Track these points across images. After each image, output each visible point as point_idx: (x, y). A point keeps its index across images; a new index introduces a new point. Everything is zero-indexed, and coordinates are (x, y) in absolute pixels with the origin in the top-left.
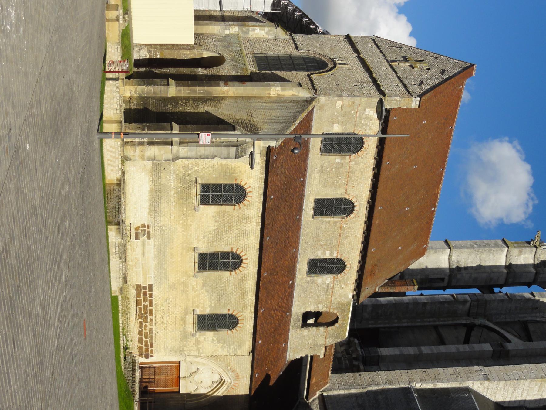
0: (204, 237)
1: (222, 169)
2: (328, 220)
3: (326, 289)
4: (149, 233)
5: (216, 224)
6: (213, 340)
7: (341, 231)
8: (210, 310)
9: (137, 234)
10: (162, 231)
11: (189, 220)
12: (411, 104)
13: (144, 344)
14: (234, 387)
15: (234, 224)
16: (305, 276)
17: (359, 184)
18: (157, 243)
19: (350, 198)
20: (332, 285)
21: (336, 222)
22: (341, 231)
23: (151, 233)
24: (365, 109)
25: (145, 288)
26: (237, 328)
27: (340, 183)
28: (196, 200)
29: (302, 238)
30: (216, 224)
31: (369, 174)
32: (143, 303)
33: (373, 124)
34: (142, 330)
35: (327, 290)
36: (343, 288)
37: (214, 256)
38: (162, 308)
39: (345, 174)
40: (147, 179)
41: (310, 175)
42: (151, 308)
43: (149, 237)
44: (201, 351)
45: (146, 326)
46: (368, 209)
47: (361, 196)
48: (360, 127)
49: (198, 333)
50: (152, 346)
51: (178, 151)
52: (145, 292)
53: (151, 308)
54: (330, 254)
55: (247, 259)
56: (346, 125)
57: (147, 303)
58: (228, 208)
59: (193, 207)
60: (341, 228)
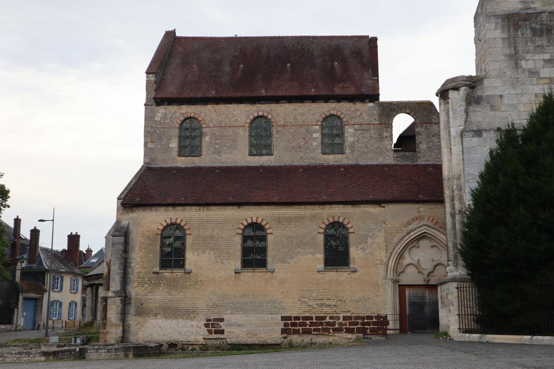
0: (223, 263)
1: (144, 248)
2: (275, 140)
3: (362, 132)
4: (215, 320)
5: (207, 252)
6: (361, 249)
7: (288, 126)
8: (319, 253)
9: (216, 332)
10: (215, 306)
11: (202, 279)
12: (151, 81)
13: (367, 327)
14: (435, 222)
15: (208, 233)
16: (344, 155)
17: (234, 116)
18: (229, 312)
19: (248, 121)
20: (356, 126)
21: (278, 132)
22: (288, 126)
23: (215, 317)
24: (156, 121)
25: (286, 325)
26: (345, 223)
27: (232, 134)
28: (178, 273)
29: (296, 163)
30: (207, 252)
31: (222, 107)
32: (308, 327)
33: (170, 112)
34: (345, 328)
35: (364, 130)
36: (361, 114)
37: (246, 251)
38: (316, 306)
39: (223, 130)
40: (152, 321)
41: (223, 163)
42: (314, 318)
43: (222, 320)
44: (379, 262)
45: (340, 324)
46: (262, 102)
47: (248, 112)
48: (173, 123)
49: (352, 266)
50: (368, 317)
51: (114, 292)
52: (291, 325)
53: (314, 318)
54: (316, 132)
55: (252, 218)
56: (171, 136)
57: (308, 322)
58: (189, 240)
59: (187, 275)
60: (284, 126)
